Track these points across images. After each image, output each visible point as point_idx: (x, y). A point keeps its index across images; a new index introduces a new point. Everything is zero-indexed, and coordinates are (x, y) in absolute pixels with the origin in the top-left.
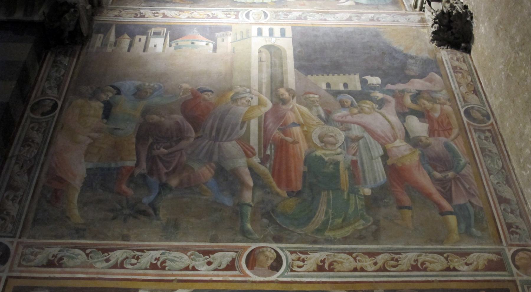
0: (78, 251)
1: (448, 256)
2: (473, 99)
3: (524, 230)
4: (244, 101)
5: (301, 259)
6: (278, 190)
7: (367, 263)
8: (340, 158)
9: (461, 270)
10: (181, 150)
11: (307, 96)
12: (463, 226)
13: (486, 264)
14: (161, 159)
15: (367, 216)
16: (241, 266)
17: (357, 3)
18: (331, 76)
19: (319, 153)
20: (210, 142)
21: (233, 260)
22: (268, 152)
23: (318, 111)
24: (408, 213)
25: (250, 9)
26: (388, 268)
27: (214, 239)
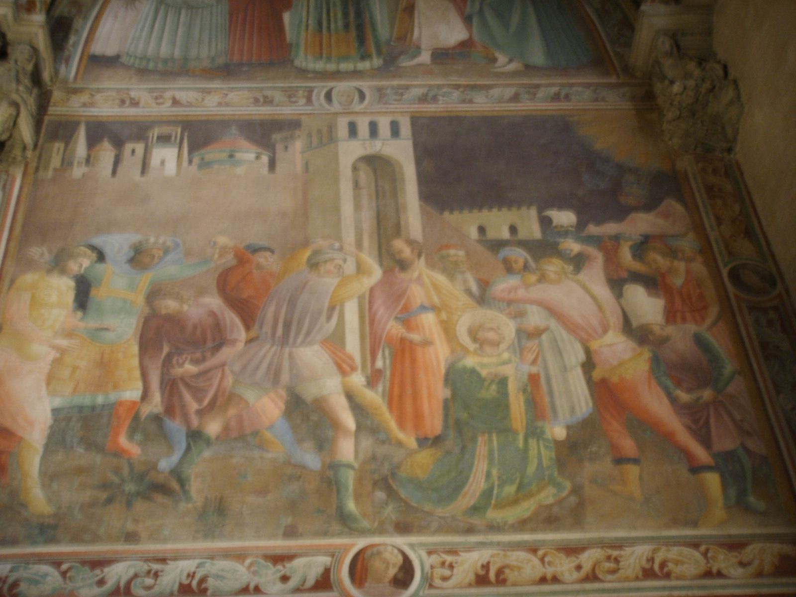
0: (45, 568)
1: (707, 550)
2: (745, 248)
4: (330, 266)
5: (447, 564)
6: (401, 435)
7: (564, 566)
8: (508, 370)
10: (223, 365)
11: (444, 252)
12: (732, 492)
14: (188, 386)
15: (560, 480)
16: (340, 582)
17: (528, 67)
18: (485, 212)
19: (470, 362)
20: (274, 349)
21: (327, 571)
22: (379, 364)
23: (465, 281)
24: (633, 471)
25: (331, 84)
26: (601, 576)
27: (291, 532)
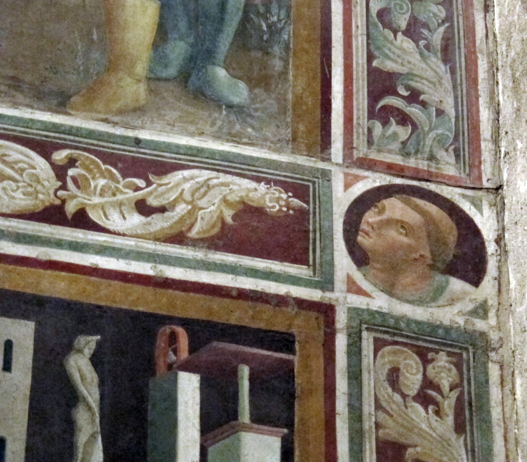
1: (72, 162)
3: (440, 113)
9: (111, 228)
13: (229, 220)
